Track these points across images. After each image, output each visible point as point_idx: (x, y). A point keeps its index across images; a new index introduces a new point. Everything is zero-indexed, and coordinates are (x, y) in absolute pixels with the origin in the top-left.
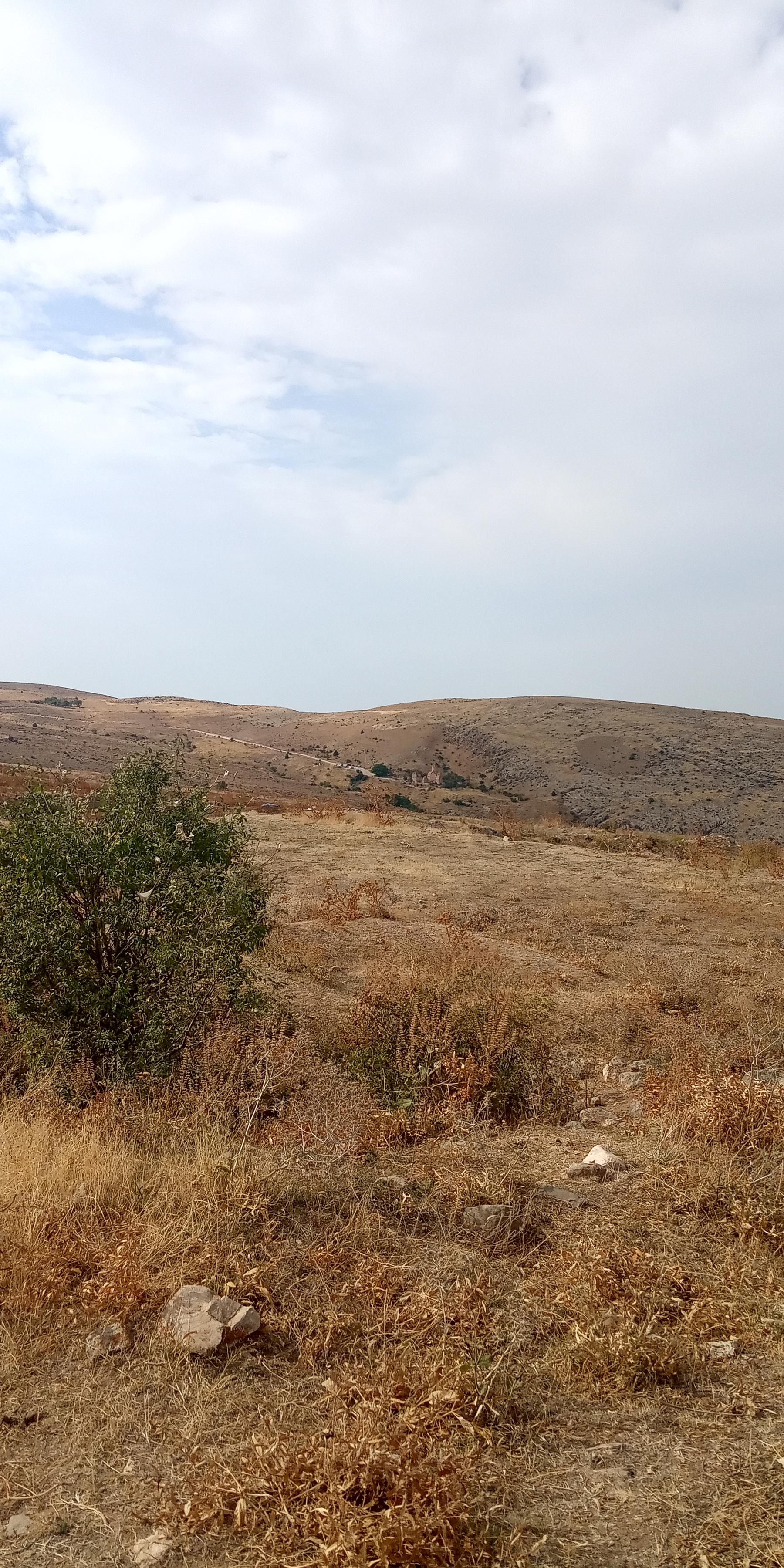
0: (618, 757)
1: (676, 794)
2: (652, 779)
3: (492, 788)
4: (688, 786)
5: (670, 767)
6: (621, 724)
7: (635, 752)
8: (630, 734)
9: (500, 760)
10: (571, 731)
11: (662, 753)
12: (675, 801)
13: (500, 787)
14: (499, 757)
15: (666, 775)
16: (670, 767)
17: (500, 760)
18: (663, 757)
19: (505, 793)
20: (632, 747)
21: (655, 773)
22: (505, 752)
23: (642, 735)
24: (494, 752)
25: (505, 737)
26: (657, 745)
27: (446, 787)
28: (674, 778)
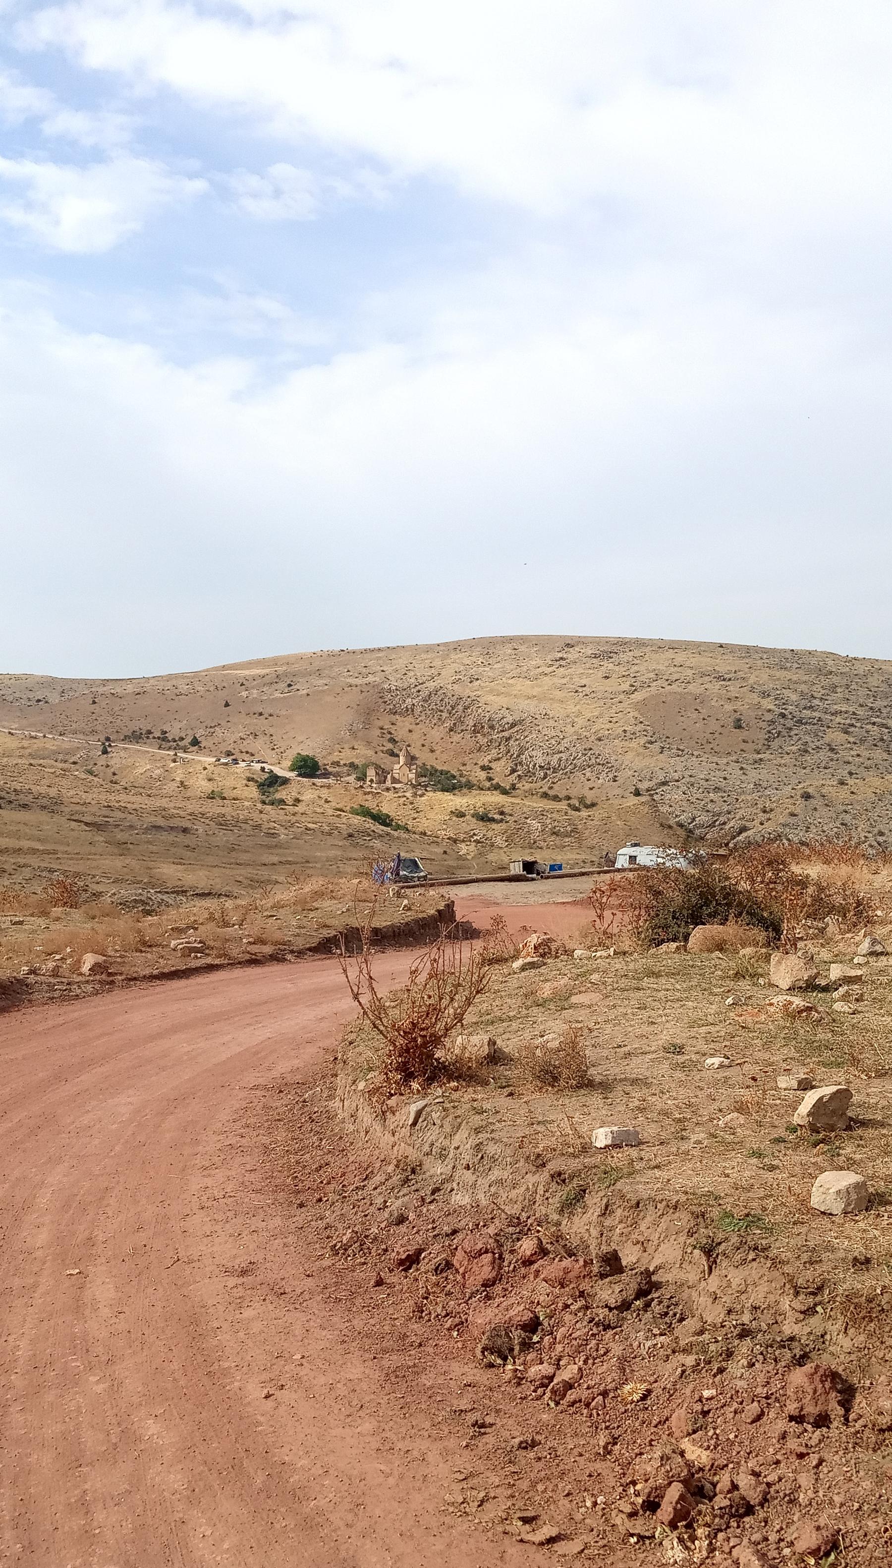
0: (714, 726)
1: (842, 783)
2: (787, 759)
3: (513, 787)
4: (853, 769)
5: (808, 738)
6: (690, 672)
7: (737, 715)
8: (715, 687)
9: (508, 739)
10: (612, 685)
11: (783, 716)
12: (843, 794)
13: (528, 786)
14: (506, 734)
15: (806, 751)
16: (808, 738)
17: (508, 739)
18: (790, 723)
19: (545, 795)
20: (729, 707)
21: (787, 749)
22: (513, 725)
23: (734, 689)
24: (492, 727)
25: (503, 701)
26: (768, 704)
27: (443, 790)
28: (824, 755)
